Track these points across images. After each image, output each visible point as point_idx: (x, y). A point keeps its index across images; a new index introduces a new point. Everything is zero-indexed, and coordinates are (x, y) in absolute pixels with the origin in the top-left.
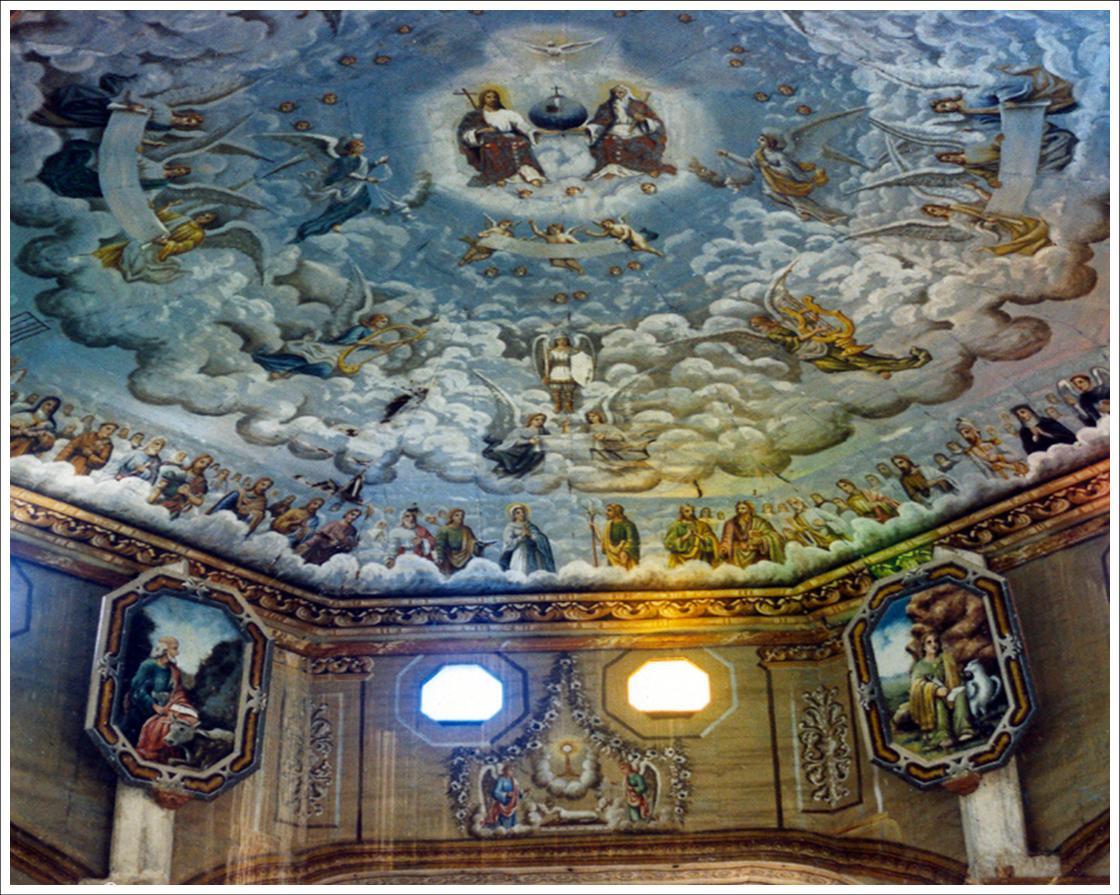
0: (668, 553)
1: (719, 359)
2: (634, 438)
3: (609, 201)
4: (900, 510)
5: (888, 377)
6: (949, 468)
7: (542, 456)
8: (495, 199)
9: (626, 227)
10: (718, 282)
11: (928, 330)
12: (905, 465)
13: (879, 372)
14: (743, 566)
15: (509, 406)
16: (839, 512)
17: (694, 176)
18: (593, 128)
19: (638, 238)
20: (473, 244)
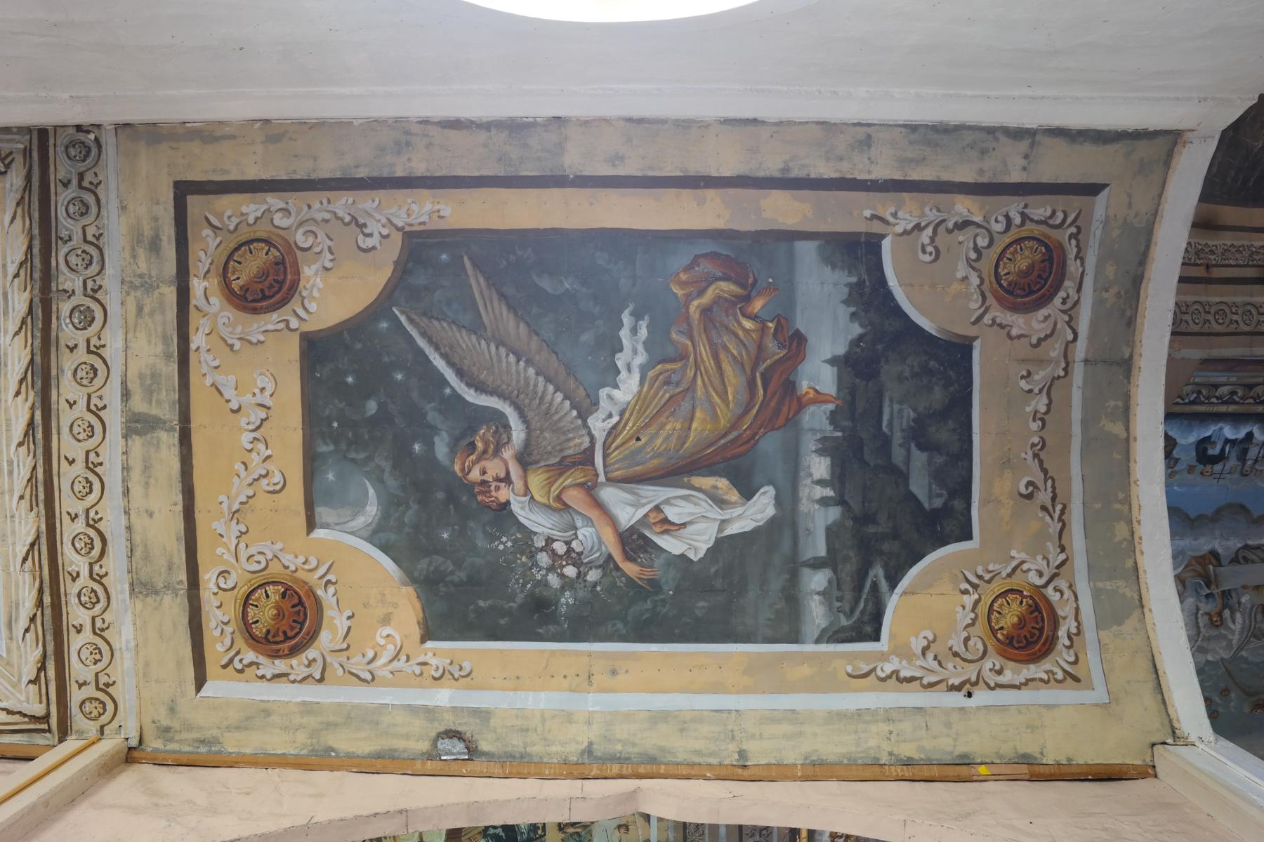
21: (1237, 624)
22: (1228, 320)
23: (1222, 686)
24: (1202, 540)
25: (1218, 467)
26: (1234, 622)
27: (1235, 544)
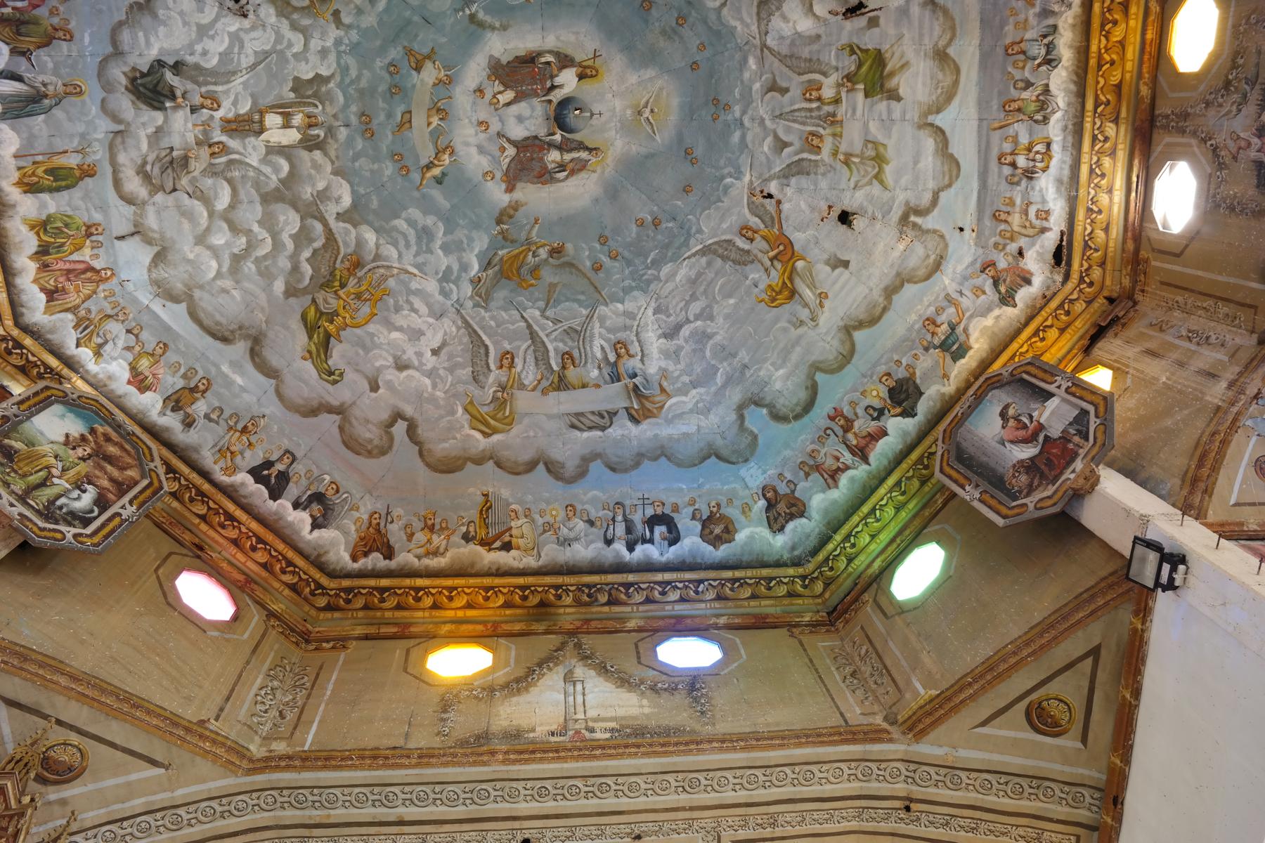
0: (44, 217)
1: (302, 237)
2: (193, 181)
3: (474, 150)
4: (148, 394)
5: (304, 359)
6: (211, 420)
7: (161, 108)
8: (474, 71)
9: (447, 162)
10: (395, 229)
11: (367, 377)
12: (202, 387)
13: (309, 352)
14: (35, 281)
15: (229, 82)
16: (128, 348)
17: (505, 205)
18: (558, 137)
19: (436, 171)
20: (429, 57)
21: (598, 345)
22: (888, 770)
23: (601, 275)
24: (649, 434)
25: (650, 512)
26: (602, 348)
27: (615, 432)
